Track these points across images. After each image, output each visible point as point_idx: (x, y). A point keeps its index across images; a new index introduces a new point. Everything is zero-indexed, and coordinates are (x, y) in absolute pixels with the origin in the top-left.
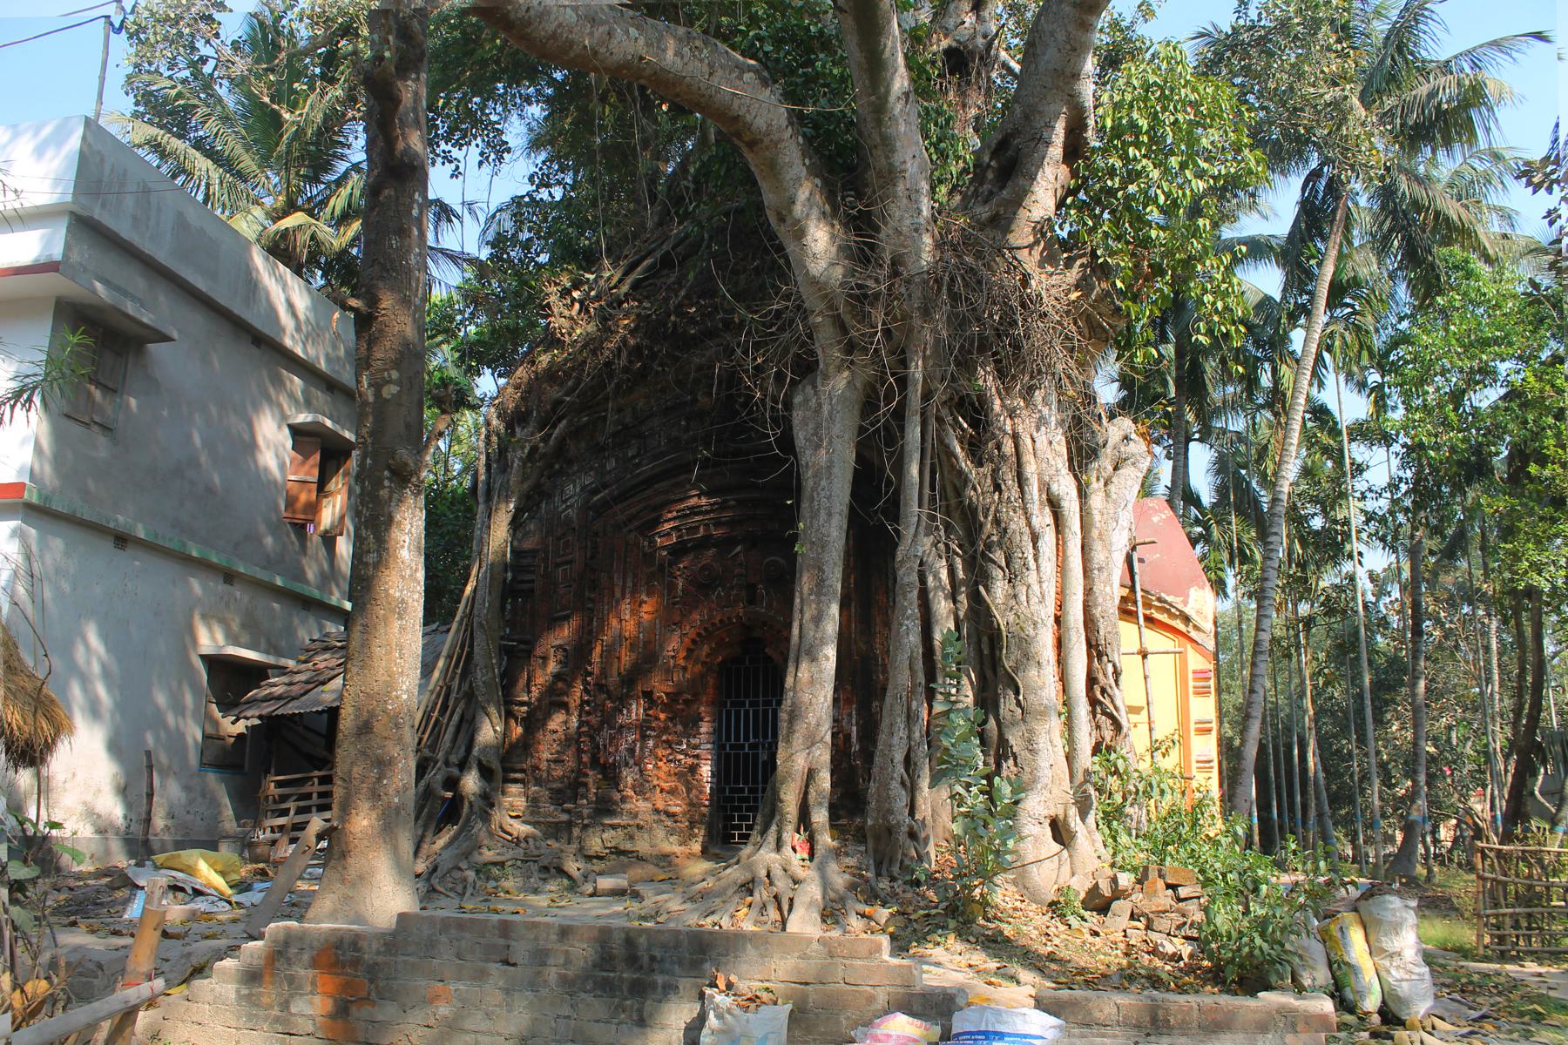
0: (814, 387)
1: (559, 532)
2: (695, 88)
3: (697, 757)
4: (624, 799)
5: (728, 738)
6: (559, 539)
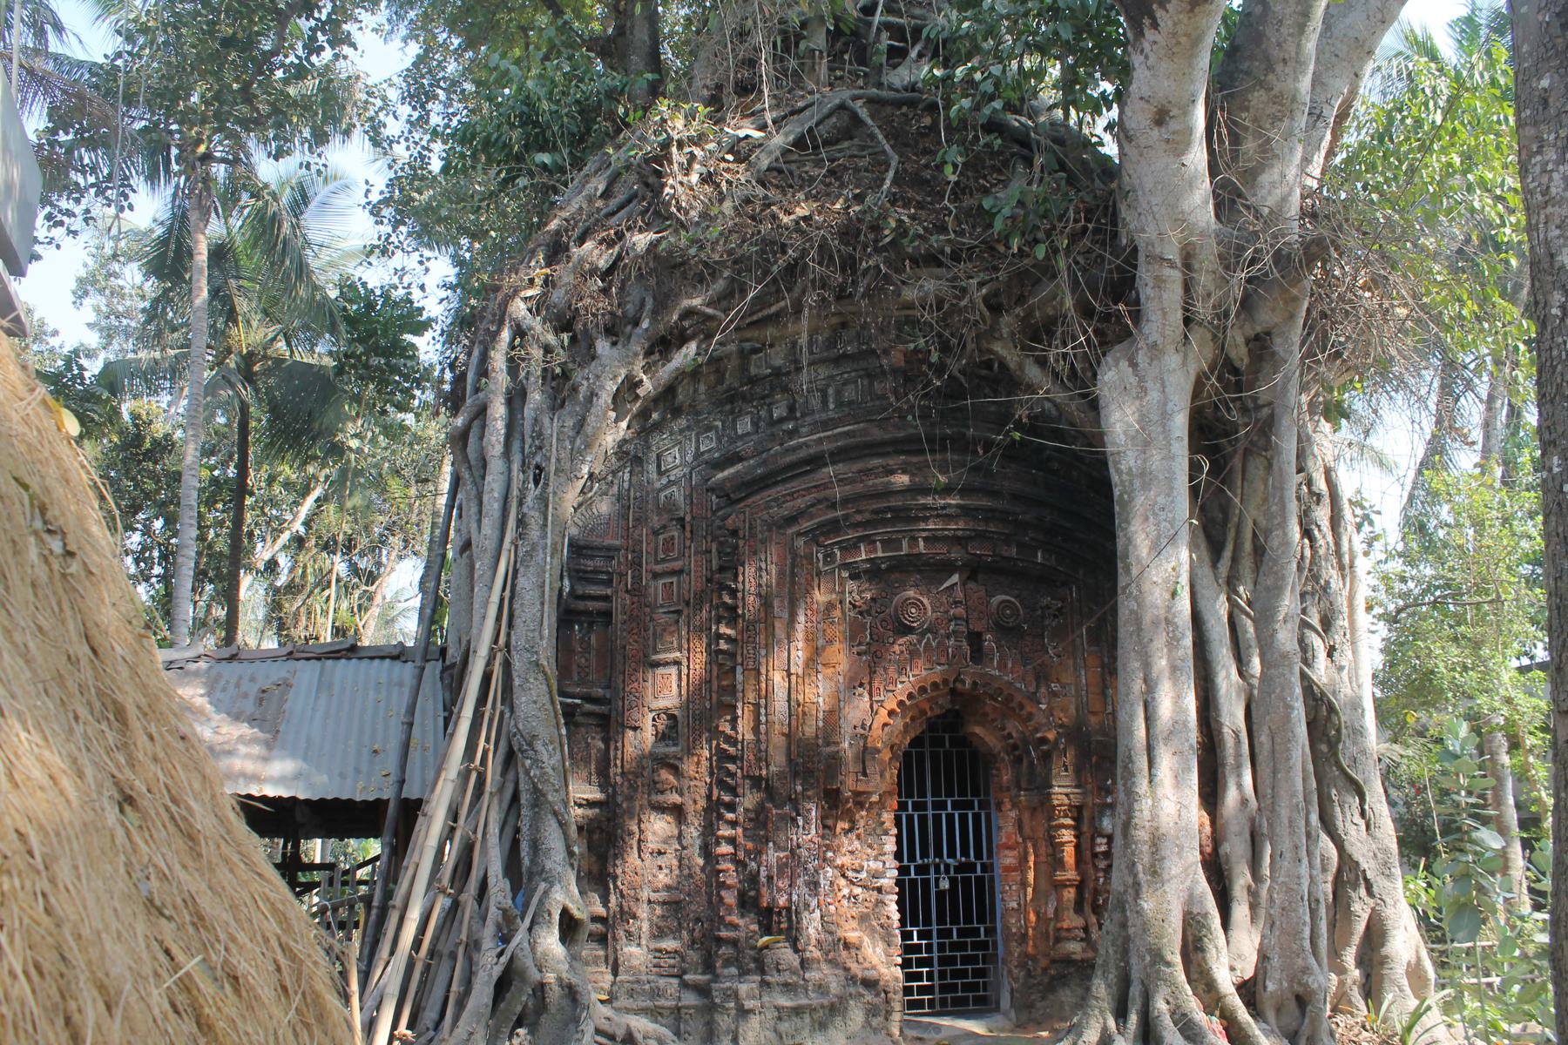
0: (1133, 364)
1: (655, 521)
3: (879, 890)
4: (805, 964)
5: (912, 858)
6: (656, 533)
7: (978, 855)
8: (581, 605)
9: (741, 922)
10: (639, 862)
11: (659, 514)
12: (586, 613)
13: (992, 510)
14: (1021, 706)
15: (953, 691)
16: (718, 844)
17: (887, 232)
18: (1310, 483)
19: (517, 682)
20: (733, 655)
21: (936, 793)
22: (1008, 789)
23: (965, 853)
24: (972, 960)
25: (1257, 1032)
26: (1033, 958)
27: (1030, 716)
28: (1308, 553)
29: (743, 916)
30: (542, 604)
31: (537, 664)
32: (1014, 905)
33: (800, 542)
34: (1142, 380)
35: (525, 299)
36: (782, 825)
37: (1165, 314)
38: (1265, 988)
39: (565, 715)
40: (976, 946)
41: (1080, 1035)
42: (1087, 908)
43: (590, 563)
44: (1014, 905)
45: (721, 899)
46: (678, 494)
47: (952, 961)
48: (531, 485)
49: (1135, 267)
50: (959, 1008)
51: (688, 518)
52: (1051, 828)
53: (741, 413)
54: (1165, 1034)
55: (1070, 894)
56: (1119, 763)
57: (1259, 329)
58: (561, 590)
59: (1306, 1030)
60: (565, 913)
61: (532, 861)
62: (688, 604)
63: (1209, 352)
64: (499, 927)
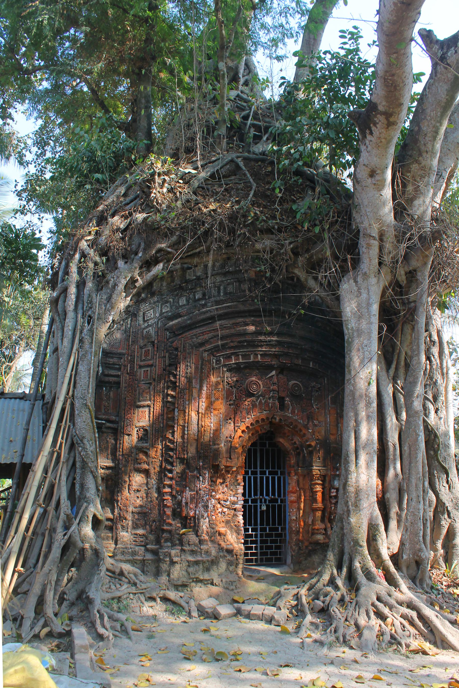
0: (356, 282)
1: (141, 343)
2: (404, 75)
3: (235, 510)
4: (201, 542)
5: (250, 496)
6: (141, 348)
7: (279, 495)
8: (107, 379)
9: (173, 523)
10: (128, 494)
11: (143, 339)
12: (109, 382)
13: (291, 343)
14: (301, 430)
15: (271, 423)
16: (164, 487)
17: (249, 218)
18: (430, 336)
19: (76, 412)
20: (173, 404)
21: (262, 467)
22: (293, 467)
23: (273, 494)
24: (276, 541)
25: (398, 577)
26: (302, 541)
27: (304, 435)
28: (428, 367)
29: (174, 520)
30: (89, 378)
31: (86, 405)
32: (294, 518)
33: (205, 354)
34: (359, 289)
35: (87, 241)
36: (193, 480)
37: (370, 260)
38: (402, 557)
39: (98, 428)
40: (277, 535)
41: (321, 576)
42: (326, 520)
43: (111, 360)
44: (294, 518)
45: (165, 512)
46: (152, 331)
47: (266, 542)
48: (86, 324)
49: (358, 239)
50: (269, 563)
51: (156, 342)
52: (312, 484)
53: (181, 296)
54: (358, 577)
55: (319, 514)
56: (343, 457)
57: (411, 268)
58: (98, 372)
59: (419, 576)
60: (95, 516)
61: (80, 493)
62: (154, 380)
63: (389, 278)
64: (65, 522)
